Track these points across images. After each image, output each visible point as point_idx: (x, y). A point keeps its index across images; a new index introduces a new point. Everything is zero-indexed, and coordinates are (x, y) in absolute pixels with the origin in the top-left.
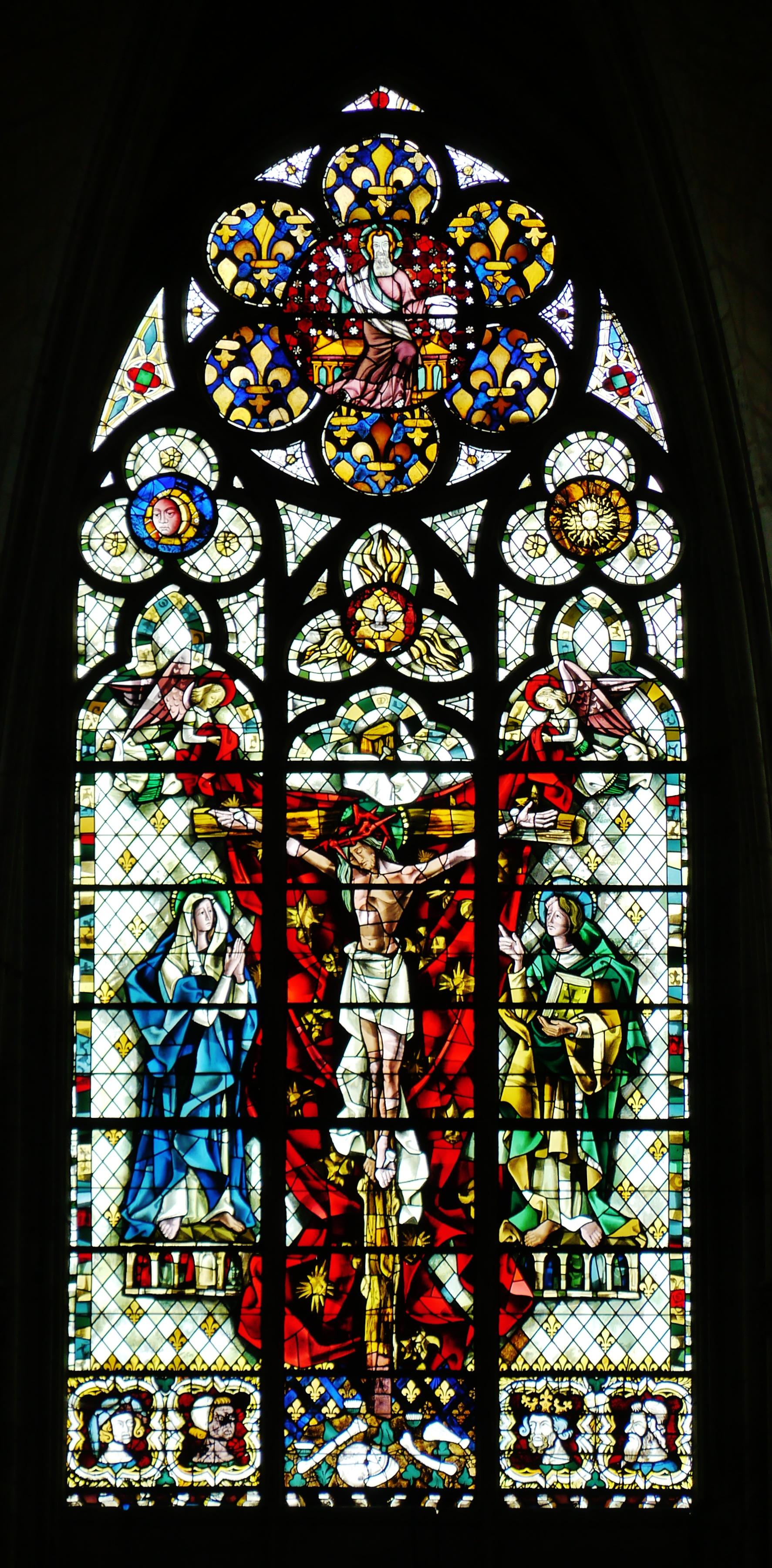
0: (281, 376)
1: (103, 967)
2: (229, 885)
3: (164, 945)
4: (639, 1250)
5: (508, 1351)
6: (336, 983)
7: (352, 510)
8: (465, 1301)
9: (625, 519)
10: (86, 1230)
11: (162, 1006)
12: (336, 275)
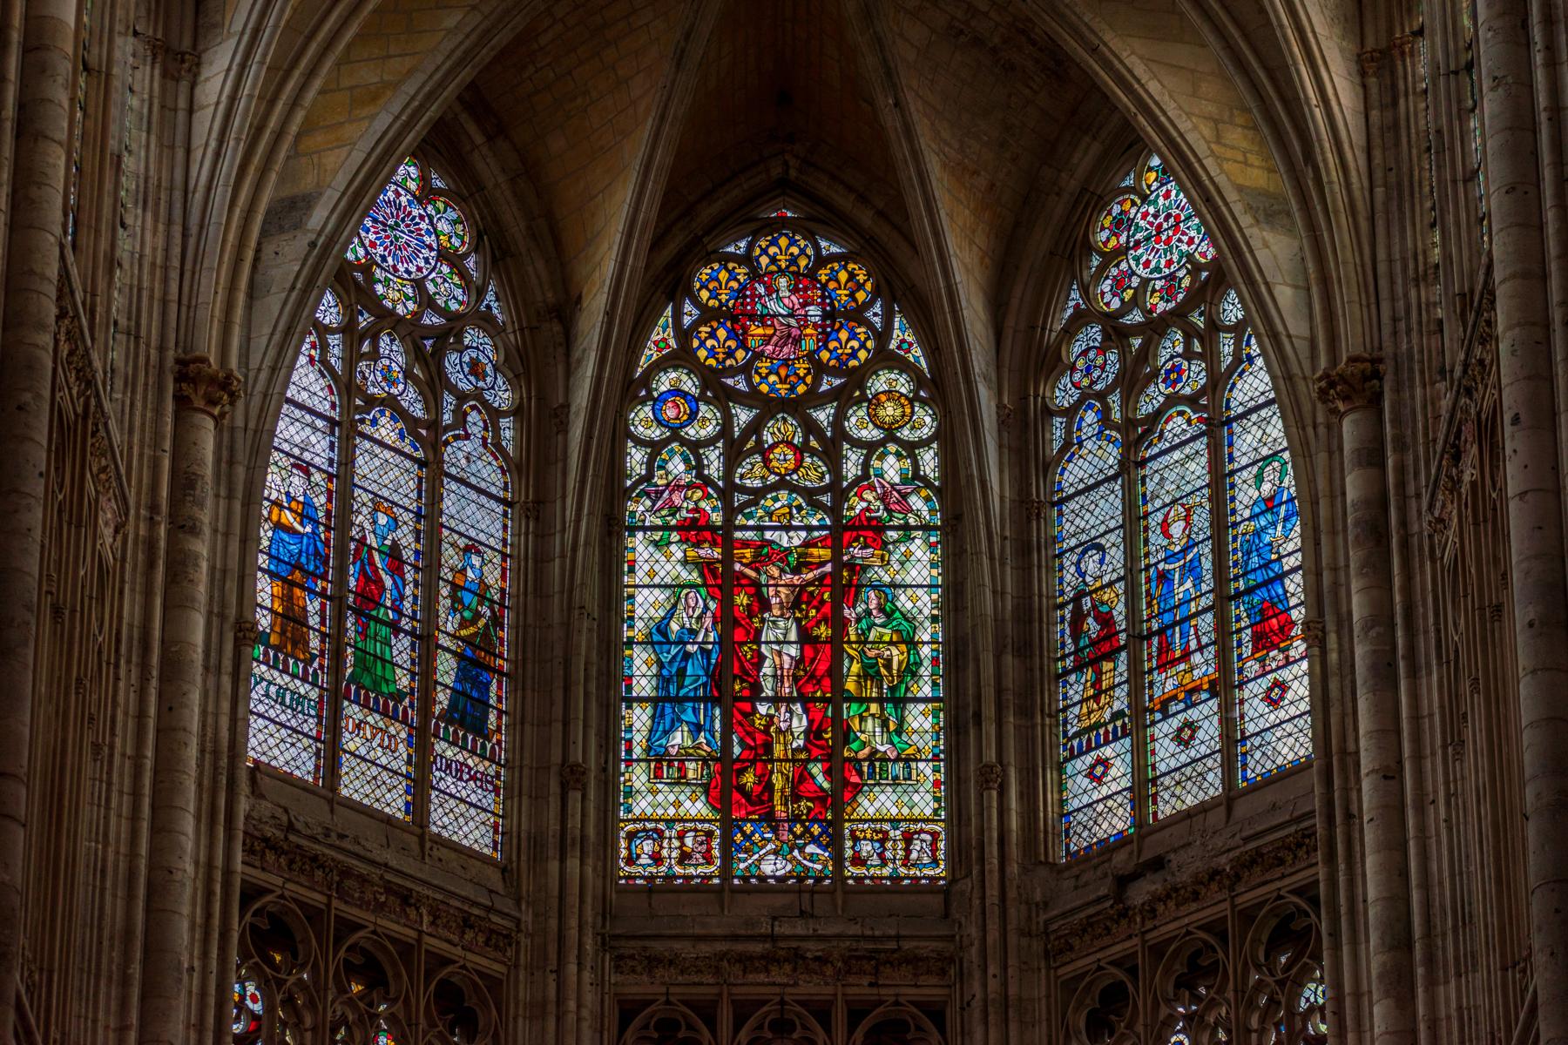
0: (732, 344)
1: (639, 624)
2: (705, 585)
3: (670, 614)
4: (917, 760)
5: (849, 809)
6: (759, 632)
7: (768, 407)
8: (826, 785)
9: (908, 411)
10: (629, 750)
11: (669, 643)
12: (760, 296)
